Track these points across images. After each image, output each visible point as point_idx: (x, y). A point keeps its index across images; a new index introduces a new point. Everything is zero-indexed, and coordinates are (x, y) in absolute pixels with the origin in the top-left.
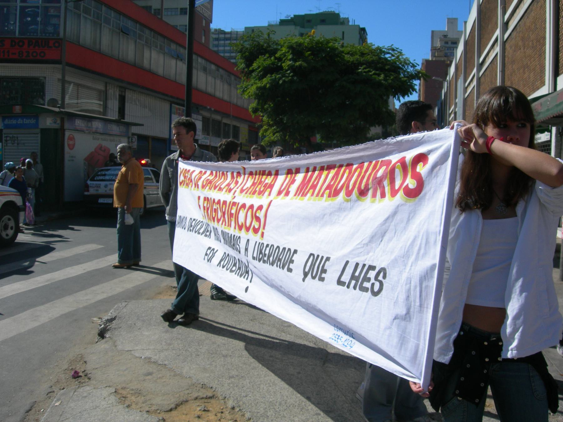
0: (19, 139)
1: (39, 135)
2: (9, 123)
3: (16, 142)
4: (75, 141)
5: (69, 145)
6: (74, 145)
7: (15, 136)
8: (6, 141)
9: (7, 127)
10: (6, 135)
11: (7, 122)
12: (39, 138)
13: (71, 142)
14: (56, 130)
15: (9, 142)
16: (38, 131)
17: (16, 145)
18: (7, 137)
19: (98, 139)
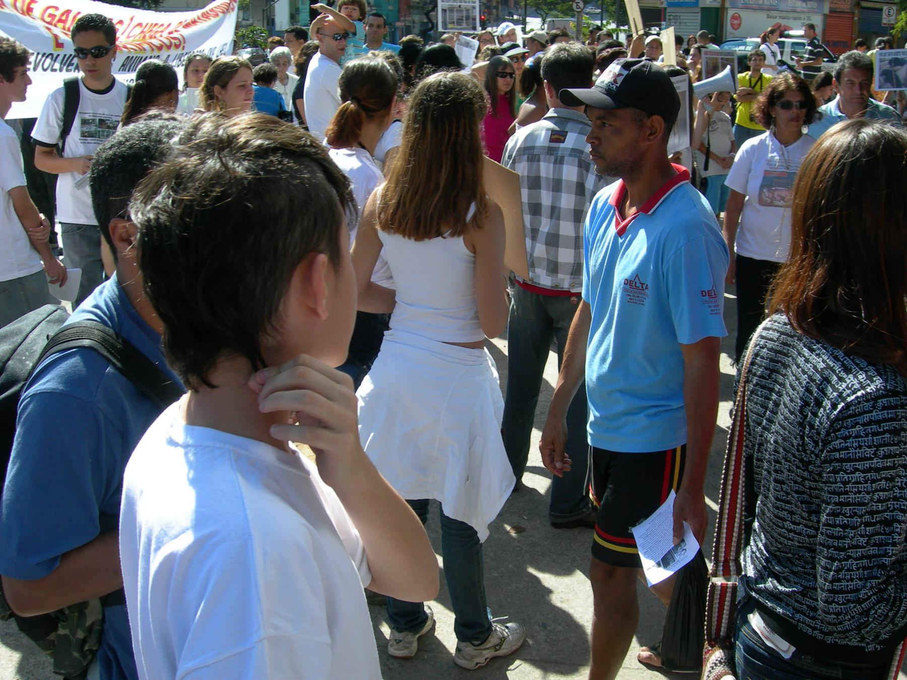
1: (699, 15)
3: (678, 21)
4: (741, 20)
5: (732, 25)
6: (739, 25)
7: (677, 14)
8: (670, 20)
12: (699, 18)
13: (736, 22)
14: (717, 9)
15: (672, 21)
16: (699, 10)
17: (678, 24)
18: (670, 15)
19: (776, 18)
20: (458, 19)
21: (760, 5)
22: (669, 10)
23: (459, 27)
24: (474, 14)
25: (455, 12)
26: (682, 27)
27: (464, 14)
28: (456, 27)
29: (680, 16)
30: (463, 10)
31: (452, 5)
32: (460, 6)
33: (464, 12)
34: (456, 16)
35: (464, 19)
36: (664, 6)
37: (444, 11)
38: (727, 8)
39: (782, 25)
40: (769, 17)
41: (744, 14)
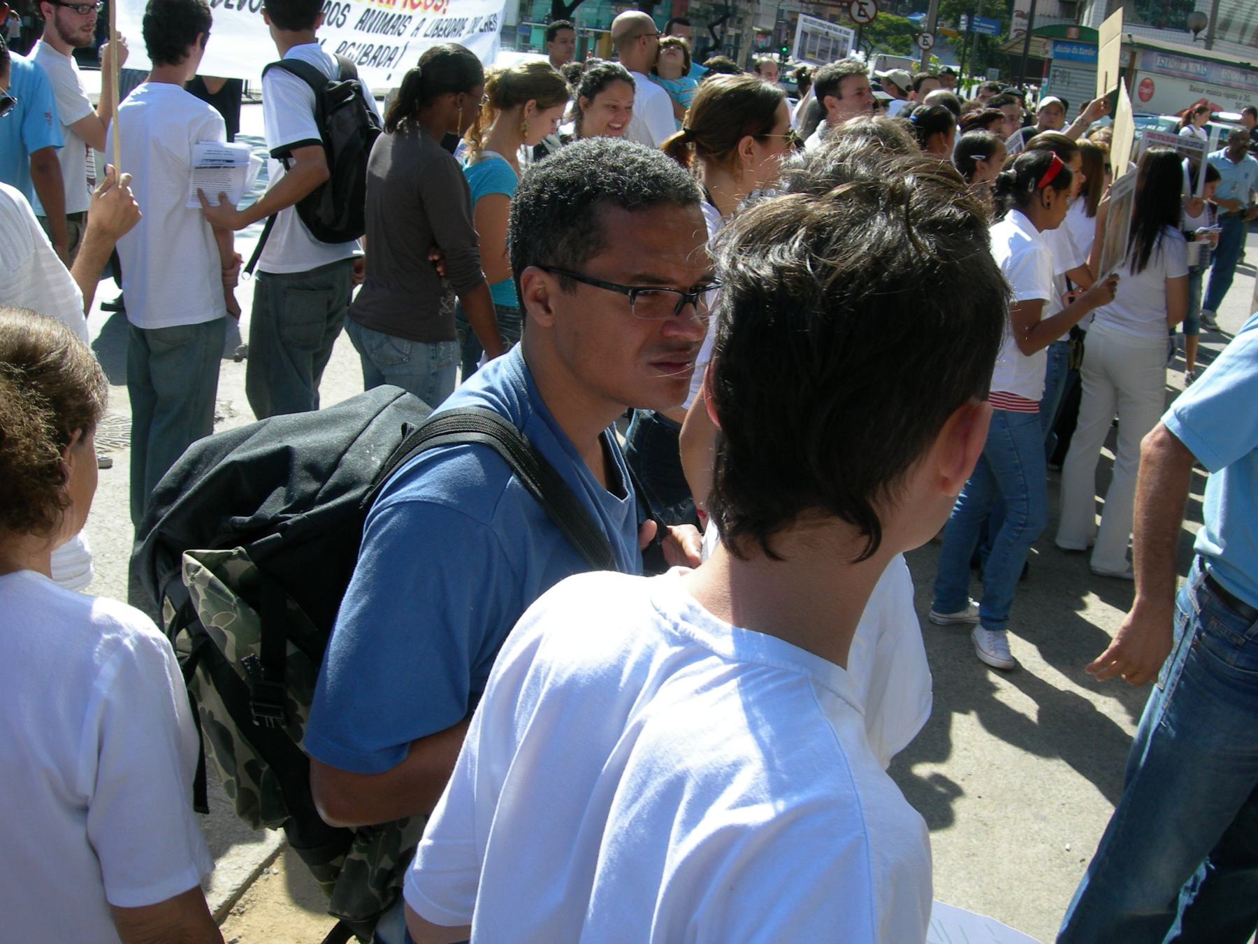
0: (1071, 75)
2: (1062, 51)
3: (1066, 79)
4: (1153, 89)
6: (1151, 95)
7: (1066, 70)
8: (1054, 76)
9: (1059, 56)
10: (1055, 68)
11: (1059, 49)
13: (1146, 91)
15: (1057, 78)
17: (1065, 83)
18: (1056, 71)
19: (1201, 91)
20: (821, 50)
21: (1182, 71)
22: (1054, 63)
23: (820, 60)
24: (845, 49)
25: (819, 40)
26: (1070, 89)
27: (831, 45)
28: (816, 59)
29: (1069, 73)
30: (829, 40)
31: (817, 29)
32: (827, 33)
33: (832, 43)
34: (819, 45)
35: (830, 52)
36: (1049, 56)
37: (804, 34)
38: (1136, 70)
39: (1209, 103)
40: (1192, 89)
41: (1159, 82)
